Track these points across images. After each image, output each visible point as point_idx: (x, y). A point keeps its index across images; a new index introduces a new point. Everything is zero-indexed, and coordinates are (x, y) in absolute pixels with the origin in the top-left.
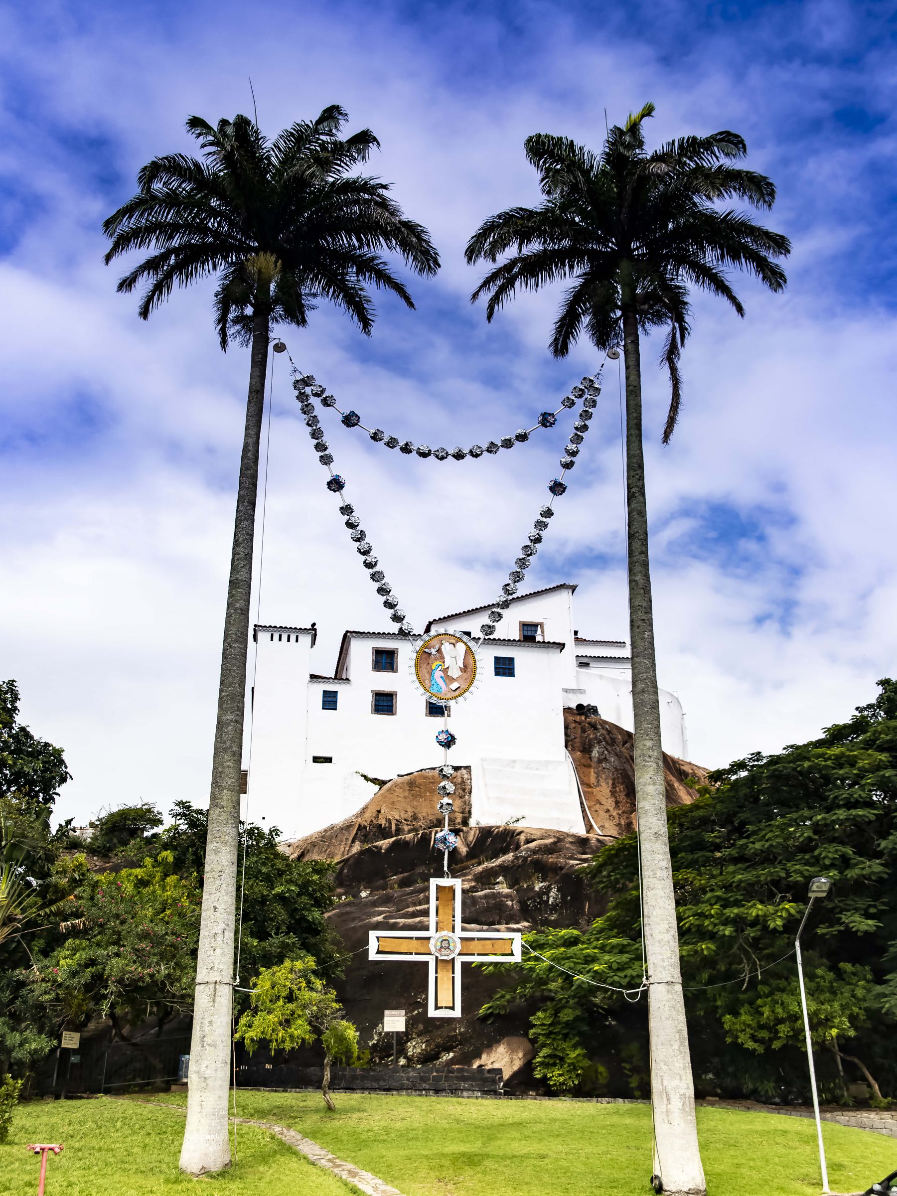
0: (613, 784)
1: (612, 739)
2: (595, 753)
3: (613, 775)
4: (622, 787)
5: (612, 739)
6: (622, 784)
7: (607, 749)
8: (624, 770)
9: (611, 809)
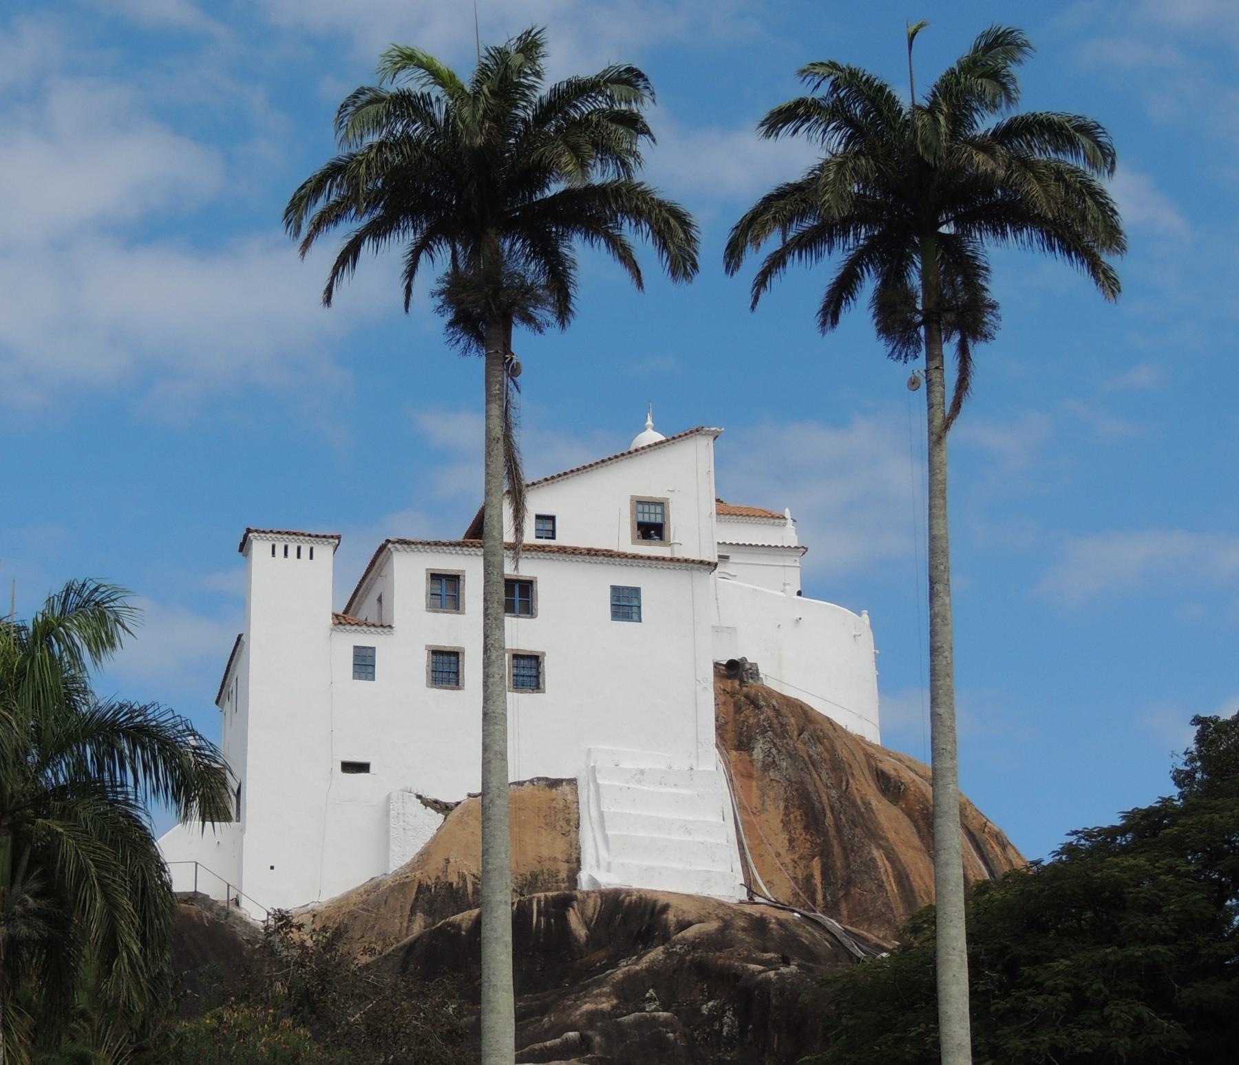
0: (786, 808)
1: (782, 725)
2: (758, 753)
3: (786, 792)
4: (798, 813)
5: (782, 725)
6: (799, 808)
7: (775, 745)
8: (802, 783)
9: (783, 852)
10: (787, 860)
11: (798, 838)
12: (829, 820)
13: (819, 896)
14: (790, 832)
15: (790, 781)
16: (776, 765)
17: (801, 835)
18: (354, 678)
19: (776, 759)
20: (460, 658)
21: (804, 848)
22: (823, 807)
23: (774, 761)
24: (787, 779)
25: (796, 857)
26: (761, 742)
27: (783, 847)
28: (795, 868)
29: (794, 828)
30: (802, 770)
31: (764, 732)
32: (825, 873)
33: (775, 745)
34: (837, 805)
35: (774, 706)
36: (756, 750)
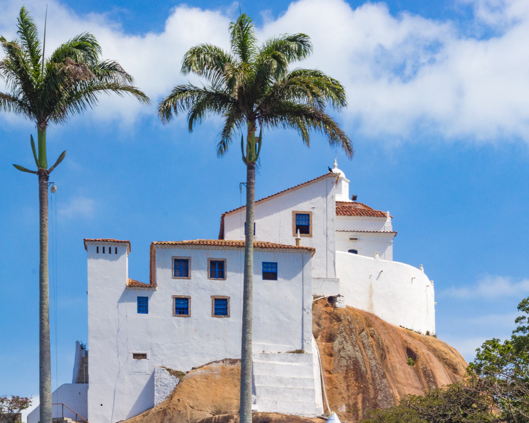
0: (347, 370)
3: (347, 362)
4: (353, 372)
7: (345, 339)
8: (356, 358)
10: (345, 396)
11: (351, 385)
12: (369, 376)
13: (360, 413)
14: (348, 382)
15: (350, 357)
16: (344, 349)
17: (353, 383)
18: (138, 313)
19: (344, 347)
20: (189, 301)
21: (354, 389)
22: (366, 370)
23: (343, 347)
24: (348, 356)
25: (350, 394)
26: (339, 338)
27: (343, 389)
28: (349, 399)
29: (350, 380)
30: (357, 351)
31: (341, 332)
32: (363, 402)
33: (345, 339)
34: (374, 368)
35: (348, 319)
36: (336, 342)
